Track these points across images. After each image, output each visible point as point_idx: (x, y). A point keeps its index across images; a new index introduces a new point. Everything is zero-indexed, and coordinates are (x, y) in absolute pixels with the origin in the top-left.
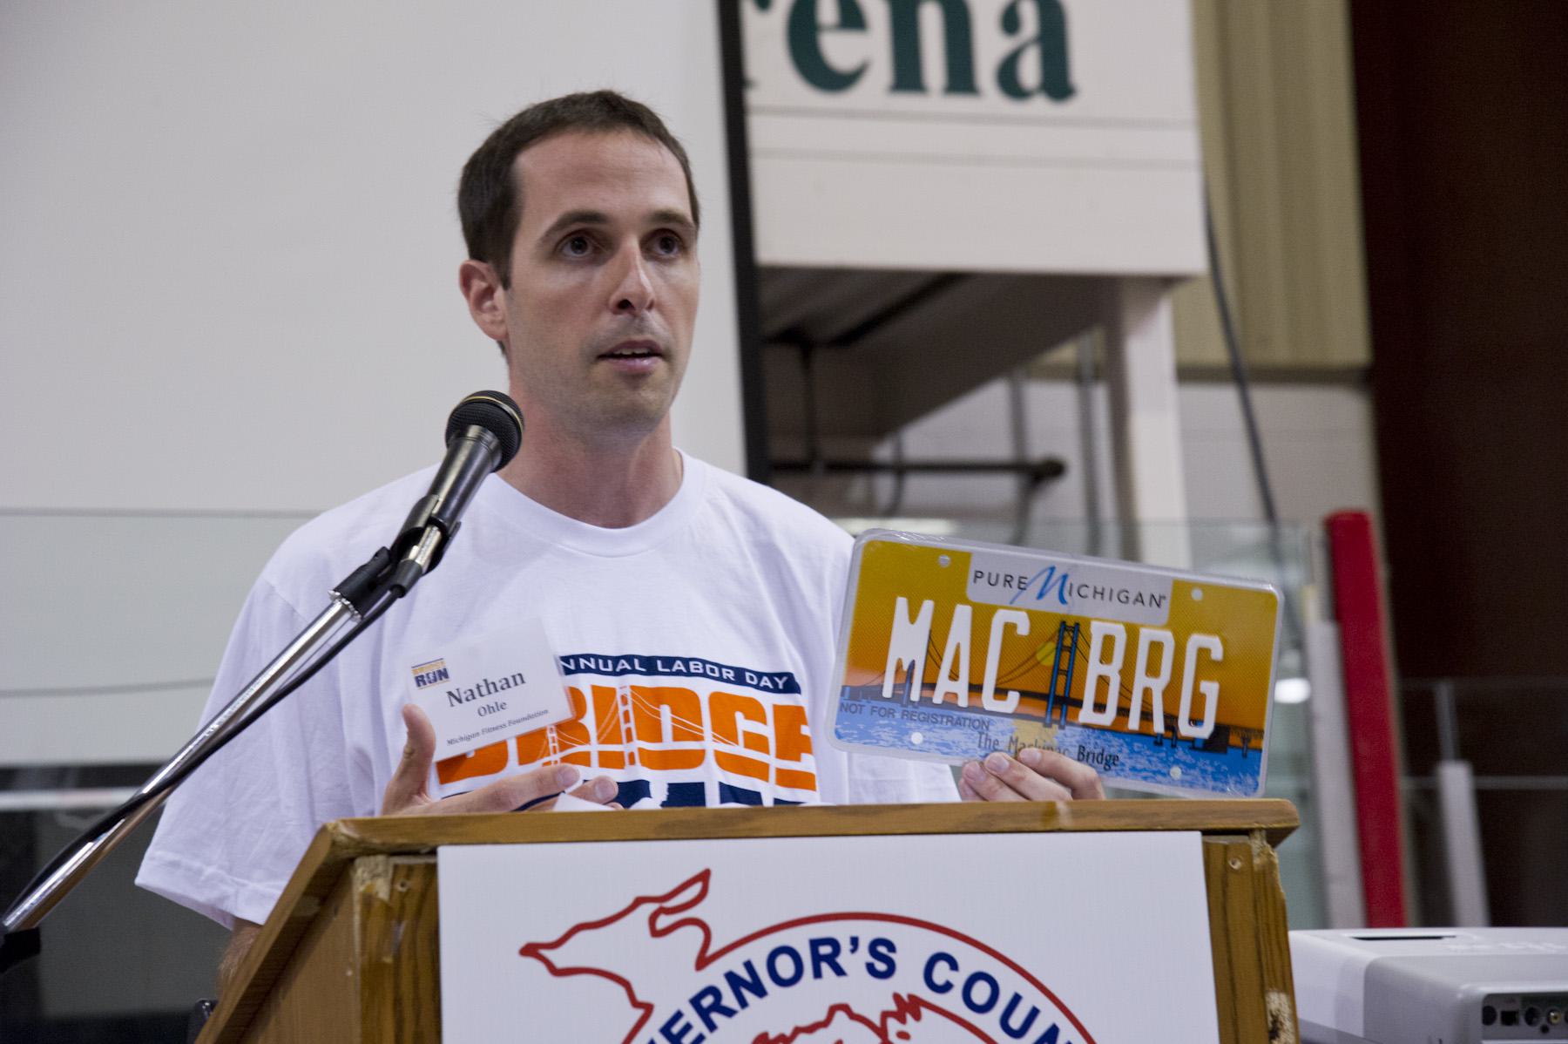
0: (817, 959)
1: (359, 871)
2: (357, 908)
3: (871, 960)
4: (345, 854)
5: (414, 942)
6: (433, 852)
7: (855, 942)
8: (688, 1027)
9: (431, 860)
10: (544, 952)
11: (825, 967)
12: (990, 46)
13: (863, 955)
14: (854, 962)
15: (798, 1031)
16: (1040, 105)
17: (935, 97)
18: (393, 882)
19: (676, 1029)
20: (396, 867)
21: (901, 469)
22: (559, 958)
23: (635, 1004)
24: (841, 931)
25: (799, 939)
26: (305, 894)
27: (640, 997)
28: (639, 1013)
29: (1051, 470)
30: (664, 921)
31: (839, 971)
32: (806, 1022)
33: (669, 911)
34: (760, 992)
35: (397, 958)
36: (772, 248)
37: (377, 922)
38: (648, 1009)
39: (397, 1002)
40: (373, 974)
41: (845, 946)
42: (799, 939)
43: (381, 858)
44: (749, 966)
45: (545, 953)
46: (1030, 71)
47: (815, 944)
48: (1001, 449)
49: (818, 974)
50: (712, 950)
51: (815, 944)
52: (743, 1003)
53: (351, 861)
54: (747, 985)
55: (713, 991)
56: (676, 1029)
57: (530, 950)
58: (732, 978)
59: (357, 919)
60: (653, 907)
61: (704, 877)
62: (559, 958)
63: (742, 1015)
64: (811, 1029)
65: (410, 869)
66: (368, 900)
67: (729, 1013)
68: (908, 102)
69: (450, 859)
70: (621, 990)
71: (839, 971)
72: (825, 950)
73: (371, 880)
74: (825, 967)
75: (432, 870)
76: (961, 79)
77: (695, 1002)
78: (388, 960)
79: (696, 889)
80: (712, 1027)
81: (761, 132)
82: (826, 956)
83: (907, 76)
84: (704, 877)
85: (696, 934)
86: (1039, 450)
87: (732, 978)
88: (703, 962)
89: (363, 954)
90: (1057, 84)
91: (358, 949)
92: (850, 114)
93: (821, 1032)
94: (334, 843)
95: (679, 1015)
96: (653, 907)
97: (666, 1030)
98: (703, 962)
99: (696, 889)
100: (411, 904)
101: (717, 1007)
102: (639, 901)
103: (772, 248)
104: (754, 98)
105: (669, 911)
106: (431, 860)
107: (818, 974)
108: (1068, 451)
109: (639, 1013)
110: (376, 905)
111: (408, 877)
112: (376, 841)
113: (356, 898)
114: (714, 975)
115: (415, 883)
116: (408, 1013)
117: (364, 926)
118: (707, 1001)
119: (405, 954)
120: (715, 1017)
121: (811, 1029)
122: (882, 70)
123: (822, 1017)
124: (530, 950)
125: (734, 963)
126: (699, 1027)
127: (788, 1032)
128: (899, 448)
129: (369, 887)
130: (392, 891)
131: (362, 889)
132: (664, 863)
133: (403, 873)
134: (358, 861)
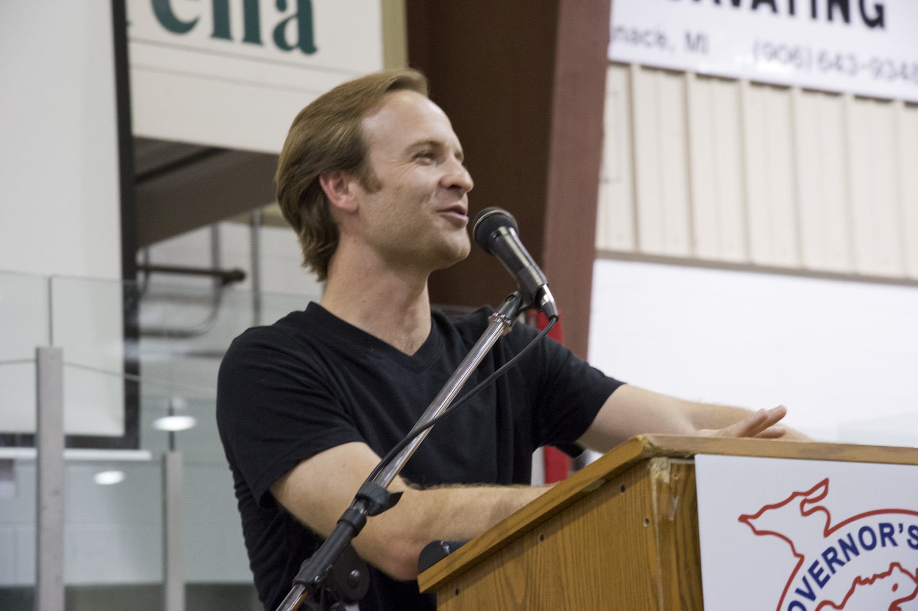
0: (883, 535)
1: (655, 465)
2: (654, 487)
3: (909, 537)
4: (648, 455)
5: (682, 510)
6: (692, 457)
7: (901, 526)
8: (821, 571)
9: (689, 462)
10: (750, 521)
11: (887, 540)
12: (269, 17)
13: (905, 535)
14: (902, 538)
15: (875, 577)
16: (297, 55)
17: (237, 44)
18: (671, 473)
19: (816, 571)
20: (672, 465)
21: (149, 269)
22: (759, 524)
23: (796, 555)
24: (894, 519)
25: (873, 522)
26: (602, 478)
27: (798, 551)
28: (797, 560)
29: (237, 276)
30: (808, 507)
31: (895, 544)
32: (879, 572)
33: (811, 500)
34: (857, 553)
35: (675, 517)
36: (142, 127)
37: (665, 496)
38: (802, 557)
39: (676, 543)
40: (665, 525)
41: (897, 529)
42: (873, 522)
43: (664, 459)
44: (849, 536)
45: (750, 521)
46: (292, 34)
47: (882, 526)
48: (204, 261)
49: (884, 544)
50: (831, 526)
51: (882, 526)
52: (848, 559)
53: (648, 459)
54: (849, 547)
55: (831, 549)
56: (816, 571)
57: (744, 519)
58: (841, 542)
59: (654, 494)
60: (799, 499)
61: (825, 482)
62: (759, 524)
63: (848, 565)
64: (882, 576)
65: (679, 466)
66: (660, 483)
67: (842, 563)
68: (221, 45)
69: (699, 460)
70: (788, 546)
71: (895, 544)
72: (887, 530)
73: (660, 471)
74: (887, 540)
75: (691, 469)
76: (252, 35)
77: (825, 555)
78: (672, 519)
79: (821, 490)
80: (834, 571)
81: (137, 53)
82: (887, 534)
83: (222, 30)
84: (825, 482)
85: (820, 516)
86: (228, 264)
87: (841, 542)
88: (827, 532)
89: (659, 514)
90: (307, 44)
91: (656, 512)
92: (188, 48)
93: (887, 578)
94: (645, 450)
95: (816, 563)
96: (799, 499)
97: (811, 570)
98: (827, 532)
99: (821, 490)
100: (680, 487)
101: (835, 559)
102: (795, 494)
103: (144, 126)
104: (133, 32)
105: (811, 500)
106: (689, 462)
107: (884, 544)
108: (244, 264)
109: (797, 560)
110: (664, 486)
111: (678, 470)
112: (665, 449)
113: (654, 481)
114: (833, 541)
115: (682, 475)
116: (681, 550)
117: (658, 499)
118: (830, 556)
119: (678, 519)
120: (835, 565)
121: (882, 576)
122: (206, 25)
123: (887, 569)
124: (744, 519)
125: (841, 534)
126: (827, 571)
127: (871, 577)
128: (147, 256)
129: (660, 475)
130: (671, 479)
131: (656, 476)
132: (807, 474)
133: (675, 469)
134: (653, 460)
